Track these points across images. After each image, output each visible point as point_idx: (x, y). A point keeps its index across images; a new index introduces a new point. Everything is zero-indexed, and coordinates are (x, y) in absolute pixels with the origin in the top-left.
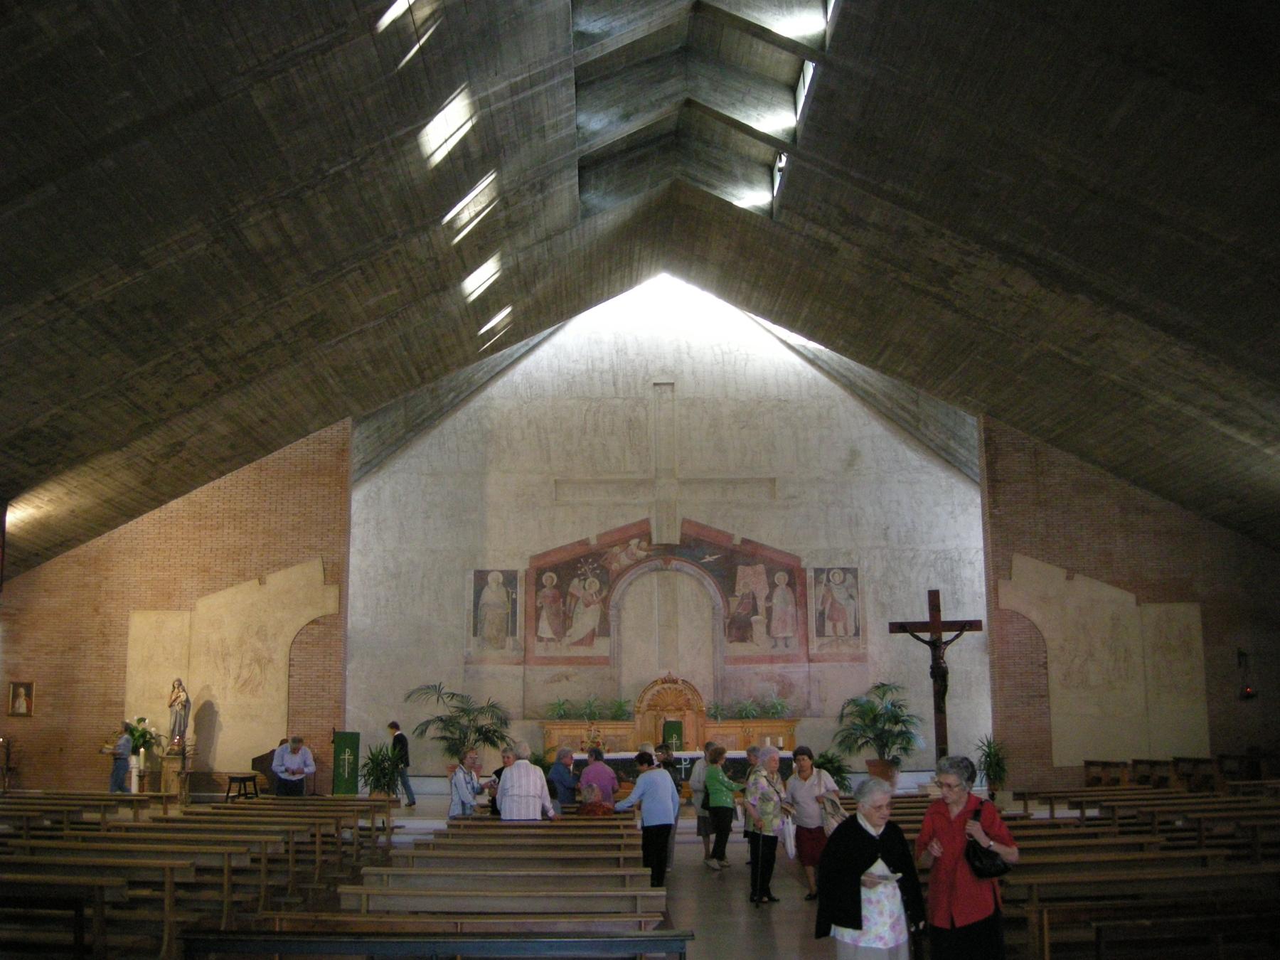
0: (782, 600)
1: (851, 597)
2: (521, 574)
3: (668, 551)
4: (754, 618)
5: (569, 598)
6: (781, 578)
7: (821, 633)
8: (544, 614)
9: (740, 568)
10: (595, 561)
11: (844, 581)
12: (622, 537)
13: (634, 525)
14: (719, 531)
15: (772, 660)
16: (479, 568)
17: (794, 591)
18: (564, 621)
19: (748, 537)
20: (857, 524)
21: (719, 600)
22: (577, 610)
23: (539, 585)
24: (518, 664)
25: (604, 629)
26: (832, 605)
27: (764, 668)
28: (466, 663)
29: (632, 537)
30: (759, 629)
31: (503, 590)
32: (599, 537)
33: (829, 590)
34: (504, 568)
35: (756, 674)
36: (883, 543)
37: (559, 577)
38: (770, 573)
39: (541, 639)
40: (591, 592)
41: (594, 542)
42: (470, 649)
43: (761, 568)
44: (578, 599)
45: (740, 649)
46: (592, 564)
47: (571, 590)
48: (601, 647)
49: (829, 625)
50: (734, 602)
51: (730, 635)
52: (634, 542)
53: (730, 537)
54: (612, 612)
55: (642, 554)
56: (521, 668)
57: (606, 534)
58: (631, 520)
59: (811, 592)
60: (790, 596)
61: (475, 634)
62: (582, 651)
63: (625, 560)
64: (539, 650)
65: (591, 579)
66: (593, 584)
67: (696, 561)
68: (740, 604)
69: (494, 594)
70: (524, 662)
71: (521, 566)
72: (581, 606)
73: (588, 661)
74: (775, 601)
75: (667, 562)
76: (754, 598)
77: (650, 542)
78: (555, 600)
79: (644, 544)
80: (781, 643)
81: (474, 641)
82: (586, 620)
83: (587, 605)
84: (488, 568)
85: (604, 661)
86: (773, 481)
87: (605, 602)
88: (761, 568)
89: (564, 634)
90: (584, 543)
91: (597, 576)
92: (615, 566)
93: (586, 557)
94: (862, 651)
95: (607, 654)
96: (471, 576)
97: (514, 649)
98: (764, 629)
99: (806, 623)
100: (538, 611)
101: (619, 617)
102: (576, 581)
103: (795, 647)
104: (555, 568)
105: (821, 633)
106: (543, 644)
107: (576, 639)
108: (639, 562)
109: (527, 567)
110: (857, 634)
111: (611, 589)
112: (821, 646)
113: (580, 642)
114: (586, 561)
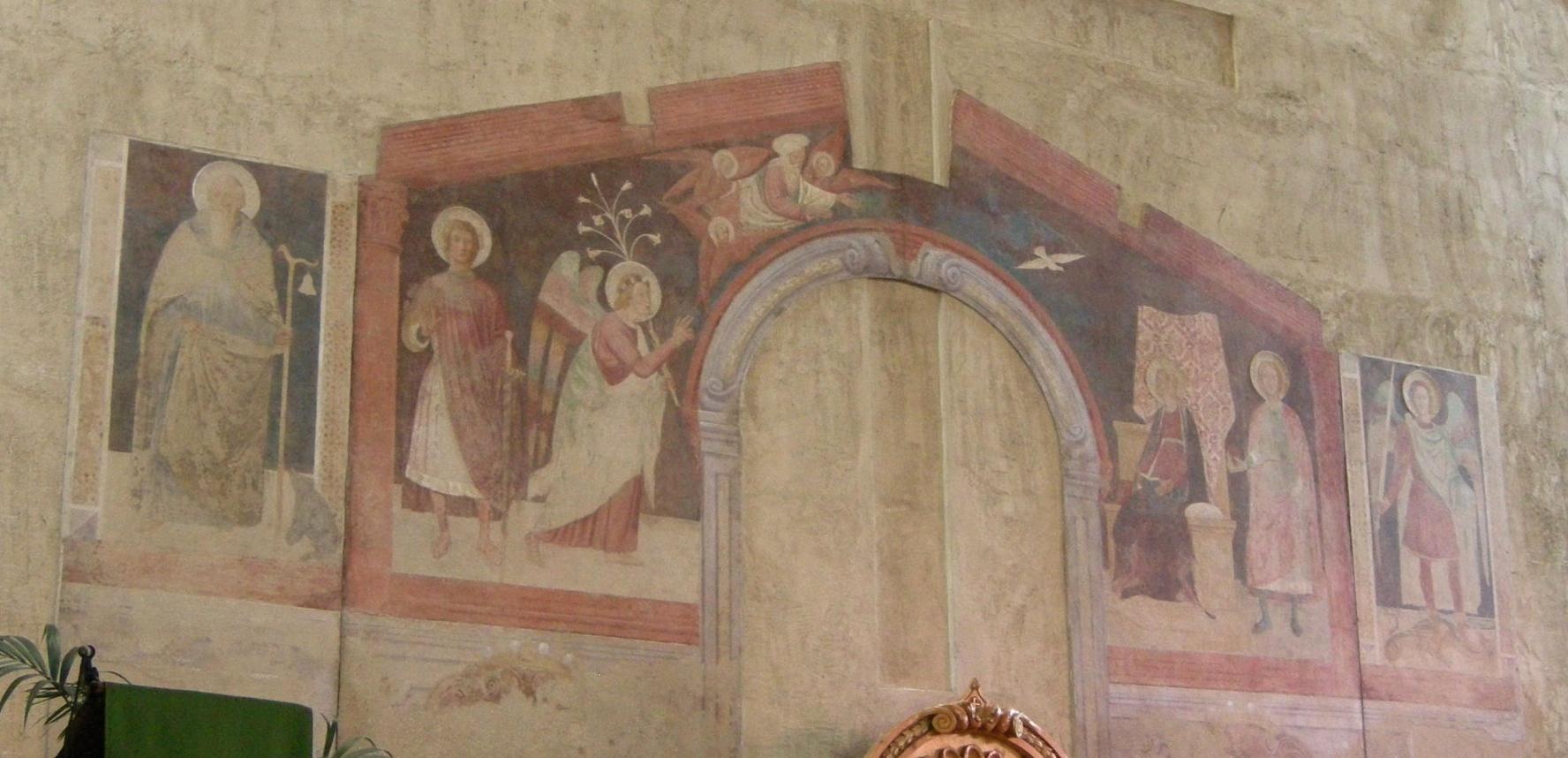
0: (1273, 455)
1: (1464, 474)
2: (340, 195)
3: (907, 199)
4: (1195, 510)
5: (539, 332)
6: (1266, 369)
7: (1389, 595)
8: (435, 385)
9: (1145, 312)
10: (644, 191)
11: (1441, 417)
12: (751, 117)
13: (788, 78)
14: (1074, 167)
15: (1253, 676)
16: (158, 140)
17: (1308, 426)
18: (519, 430)
19: (1160, 202)
20: (1465, 229)
21: (1080, 424)
22: (573, 389)
23: (419, 260)
24: (315, 602)
25: (675, 483)
26: (1414, 492)
27: (1233, 705)
28: (72, 574)
29: (787, 125)
30: (1210, 556)
31: (258, 258)
32: (657, 97)
33: (1404, 442)
34: (266, 156)
35: (1210, 726)
36: (1532, 309)
37: (499, 233)
38: (1236, 352)
39: (418, 498)
40: (634, 315)
41: (638, 115)
42: (96, 509)
43: (1206, 324)
44: (574, 341)
45: (1155, 624)
46: (630, 201)
47: (546, 297)
48: (667, 563)
49: (1410, 566)
50: (1131, 444)
51: (1122, 567)
52: (789, 145)
53: (1109, 195)
54: (709, 418)
55: (819, 198)
56: (329, 618)
57: (686, 92)
58: (774, 63)
59: (1354, 440)
60: (1299, 449)
61: (120, 442)
62: (589, 572)
63: (755, 212)
64: (410, 547)
65: (628, 265)
66: (637, 290)
67: (1003, 259)
68: (1151, 449)
69: (211, 261)
70: (342, 595)
71: (343, 164)
72: (585, 371)
73: (615, 618)
74: (1254, 455)
75: (906, 249)
76: (1193, 436)
77: (845, 158)
78: (482, 333)
79: (825, 162)
80: (1278, 618)
81: (111, 468)
82: (608, 437)
83: (613, 375)
84: (193, 139)
85: (678, 625)
86: (1227, 23)
87: (683, 367)
88: (1206, 324)
89: (520, 483)
90: (604, 110)
91: (648, 255)
92: (719, 228)
93: (612, 170)
94: (1501, 672)
95: (688, 593)
96: (114, 163)
97: (298, 530)
98: (1226, 560)
99: (1347, 550)
100: (410, 369)
101: (734, 440)
102: (567, 264)
103: (1319, 646)
104: (484, 195)
105: (1389, 595)
106: (428, 519)
107: (565, 512)
108: (806, 229)
109: (366, 167)
110: (1486, 608)
111: (705, 323)
112: (1392, 644)
113: (583, 532)
114: (610, 187)
